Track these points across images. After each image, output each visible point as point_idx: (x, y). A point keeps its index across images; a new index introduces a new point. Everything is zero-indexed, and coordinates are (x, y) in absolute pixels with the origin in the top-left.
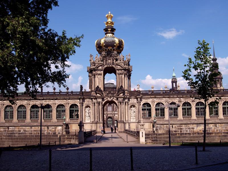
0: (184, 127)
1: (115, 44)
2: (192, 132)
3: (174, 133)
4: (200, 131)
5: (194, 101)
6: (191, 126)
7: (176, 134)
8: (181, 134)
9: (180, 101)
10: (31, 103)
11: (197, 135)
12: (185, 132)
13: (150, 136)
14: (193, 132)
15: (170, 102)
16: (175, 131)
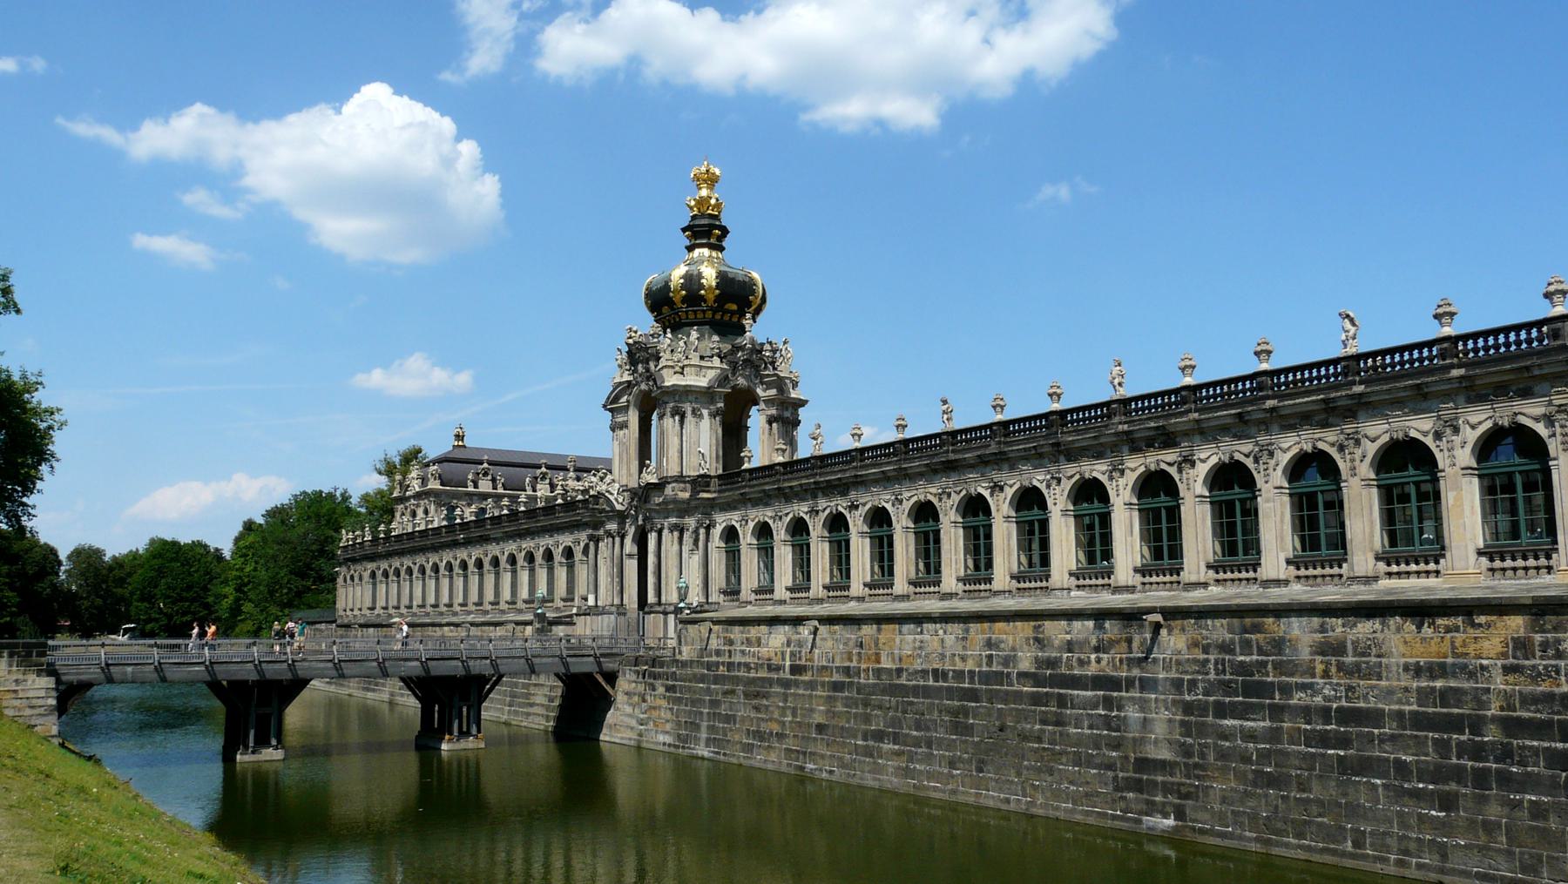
0: (736, 633)
1: (702, 292)
2: (756, 661)
3: (714, 659)
4: (776, 654)
5: (857, 507)
6: (754, 632)
7: (717, 664)
8: (730, 666)
9: (814, 512)
10: (524, 546)
11: (763, 674)
12: (737, 659)
13: (665, 669)
14: (758, 659)
15: (787, 514)
16: (718, 653)
